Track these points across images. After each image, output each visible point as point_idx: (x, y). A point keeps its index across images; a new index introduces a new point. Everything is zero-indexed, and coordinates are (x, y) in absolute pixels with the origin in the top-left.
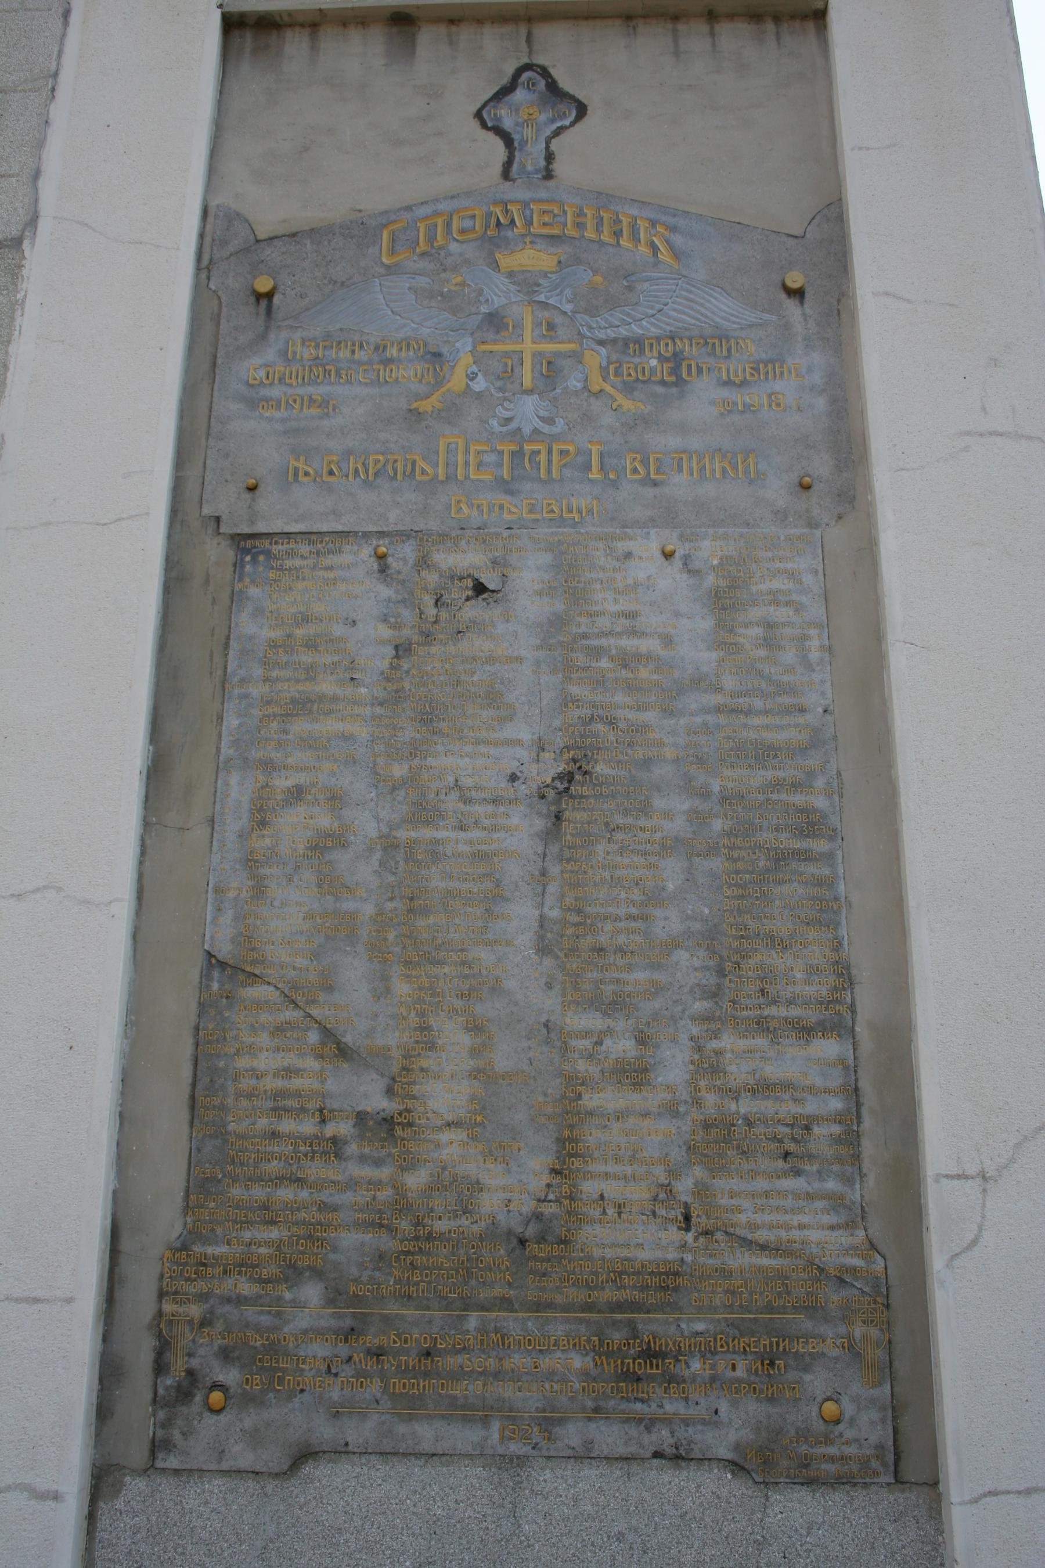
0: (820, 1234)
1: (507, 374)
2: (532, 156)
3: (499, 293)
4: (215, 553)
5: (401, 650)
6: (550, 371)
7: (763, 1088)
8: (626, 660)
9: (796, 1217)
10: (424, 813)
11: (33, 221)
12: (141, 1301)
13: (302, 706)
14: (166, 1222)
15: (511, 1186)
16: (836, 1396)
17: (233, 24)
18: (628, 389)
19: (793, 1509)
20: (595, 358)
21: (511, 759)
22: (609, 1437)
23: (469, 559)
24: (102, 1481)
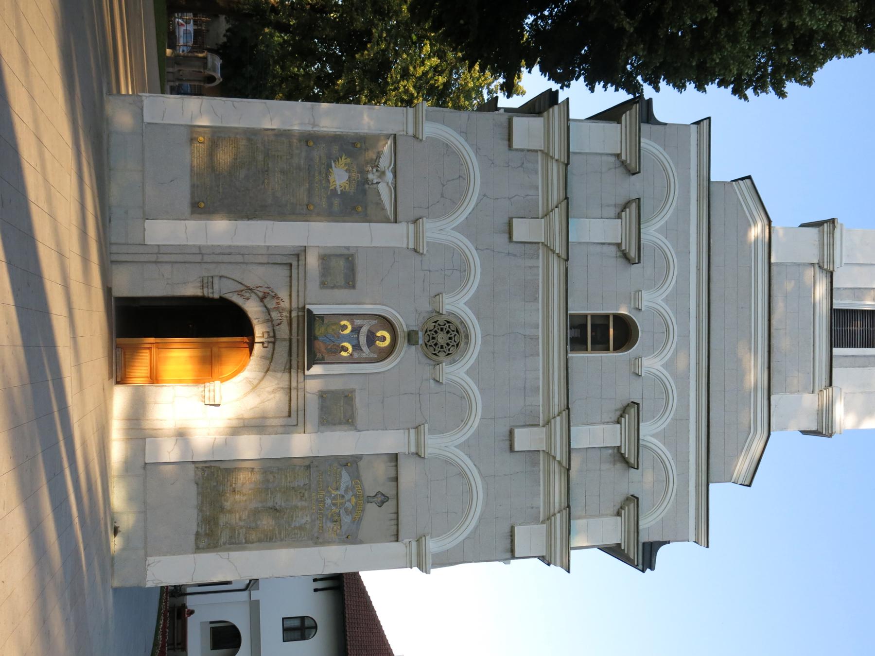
0: (223, 540)
1: (334, 498)
2: (371, 500)
3: (347, 497)
4: (307, 463)
5: (293, 488)
6: (335, 504)
7: (239, 534)
8: (292, 517)
9: (224, 537)
10: (272, 494)
11: (359, 431)
12: (213, 464)
13: (286, 476)
14: (223, 466)
15: (227, 505)
16: (203, 543)
18: (332, 515)
19: (193, 538)
20: (337, 510)
21: (279, 503)
22: (200, 517)
23: (306, 495)
24: (193, 462)
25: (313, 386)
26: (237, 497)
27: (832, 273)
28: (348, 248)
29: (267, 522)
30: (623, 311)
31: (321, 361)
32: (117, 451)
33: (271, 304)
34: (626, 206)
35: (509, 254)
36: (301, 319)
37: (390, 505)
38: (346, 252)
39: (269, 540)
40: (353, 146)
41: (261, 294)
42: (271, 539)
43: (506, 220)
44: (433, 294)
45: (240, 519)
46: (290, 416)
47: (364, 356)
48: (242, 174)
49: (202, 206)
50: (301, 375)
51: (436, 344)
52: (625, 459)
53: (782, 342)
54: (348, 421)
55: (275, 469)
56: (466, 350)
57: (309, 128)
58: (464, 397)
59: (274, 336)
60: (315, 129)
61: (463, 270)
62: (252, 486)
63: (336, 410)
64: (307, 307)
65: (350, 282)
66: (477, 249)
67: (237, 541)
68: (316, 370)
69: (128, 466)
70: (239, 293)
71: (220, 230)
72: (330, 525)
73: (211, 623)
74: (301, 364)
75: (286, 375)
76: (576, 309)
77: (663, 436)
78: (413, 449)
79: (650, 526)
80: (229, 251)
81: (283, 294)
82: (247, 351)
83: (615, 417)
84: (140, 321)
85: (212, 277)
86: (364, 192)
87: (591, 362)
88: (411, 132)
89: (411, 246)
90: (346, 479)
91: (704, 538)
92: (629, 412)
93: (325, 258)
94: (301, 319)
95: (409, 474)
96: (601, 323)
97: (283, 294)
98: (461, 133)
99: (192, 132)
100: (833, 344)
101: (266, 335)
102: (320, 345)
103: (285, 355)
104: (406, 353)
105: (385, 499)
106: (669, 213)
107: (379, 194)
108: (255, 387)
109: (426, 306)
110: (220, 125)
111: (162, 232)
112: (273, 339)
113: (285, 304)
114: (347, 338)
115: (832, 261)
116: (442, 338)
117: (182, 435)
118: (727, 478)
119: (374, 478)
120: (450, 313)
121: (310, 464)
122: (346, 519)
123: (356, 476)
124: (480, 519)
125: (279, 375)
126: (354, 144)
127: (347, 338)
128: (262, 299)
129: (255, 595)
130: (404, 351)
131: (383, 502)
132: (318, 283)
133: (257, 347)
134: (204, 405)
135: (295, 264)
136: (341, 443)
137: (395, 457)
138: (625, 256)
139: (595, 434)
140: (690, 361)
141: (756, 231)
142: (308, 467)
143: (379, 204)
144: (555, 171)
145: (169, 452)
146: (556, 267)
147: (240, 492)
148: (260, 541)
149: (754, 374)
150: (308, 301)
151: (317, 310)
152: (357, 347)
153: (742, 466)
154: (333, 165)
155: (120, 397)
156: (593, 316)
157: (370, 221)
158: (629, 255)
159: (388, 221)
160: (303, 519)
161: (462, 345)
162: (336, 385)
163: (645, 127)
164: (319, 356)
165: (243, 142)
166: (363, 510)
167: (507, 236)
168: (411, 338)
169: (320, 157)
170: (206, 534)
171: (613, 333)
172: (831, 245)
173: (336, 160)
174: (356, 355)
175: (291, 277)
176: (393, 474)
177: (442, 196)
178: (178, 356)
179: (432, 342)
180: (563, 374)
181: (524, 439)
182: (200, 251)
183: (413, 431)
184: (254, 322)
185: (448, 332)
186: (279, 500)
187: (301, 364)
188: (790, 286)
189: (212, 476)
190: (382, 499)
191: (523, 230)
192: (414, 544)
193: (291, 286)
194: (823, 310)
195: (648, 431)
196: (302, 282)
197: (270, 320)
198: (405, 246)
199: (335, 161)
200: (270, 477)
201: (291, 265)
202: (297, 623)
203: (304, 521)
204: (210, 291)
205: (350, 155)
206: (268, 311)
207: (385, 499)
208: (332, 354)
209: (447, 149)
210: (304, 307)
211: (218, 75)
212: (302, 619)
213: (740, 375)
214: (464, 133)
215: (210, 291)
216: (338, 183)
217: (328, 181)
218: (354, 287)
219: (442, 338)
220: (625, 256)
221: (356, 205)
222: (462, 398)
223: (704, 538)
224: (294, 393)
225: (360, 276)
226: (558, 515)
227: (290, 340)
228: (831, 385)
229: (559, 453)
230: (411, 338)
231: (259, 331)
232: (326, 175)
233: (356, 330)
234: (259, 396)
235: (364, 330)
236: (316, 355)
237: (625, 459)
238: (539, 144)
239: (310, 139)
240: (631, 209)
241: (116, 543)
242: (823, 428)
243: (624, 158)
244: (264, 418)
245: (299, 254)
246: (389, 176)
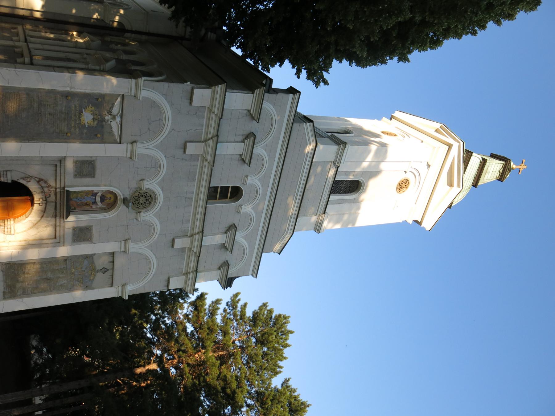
0: (18, 294)
4: (65, 258)
14: (17, 263)
17: (114, 253)
23: (65, 272)
26: (26, 276)
27: (338, 167)
28: (91, 157)
29: (43, 286)
33: (44, 185)
34: (247, 137)
35: (182, 159)
36: (62, 193)
37: (109, 273)
38: (90, 159)
41: (38, 179)
42: (45, 291)
43: (183, 142)
44: (139, 179)
45: (28, 284)
46: (55, 238)
47: (98, 207)
48: (24, 115)
50: (62, 220)
51: (139, 203)
55: (47, 264)
56: (154, 205)
57: (68, 89)
58: (151, 226)
59: (46, 200)
60: (72, 90)
62: (35, 270)
63: (82, 234)
64: (66, 189)
65: (91, 174)
66: (165, 157)
67: (25, 293)
70: (24, 179)
72: (77, 282)
74: (62, 215)
75: (53, 219)
78: (122, 250)
82: (29, 203)
83: (224, 230)
85: (6, 171)
86: (102, 127)
88: (133, 94)
89: (129, 156)
92: (232, 228)
94: (62, 193)
95: (119, 261)
98: (163, 95)
101: (41, 200)
103: (53, 209)
104: (121, 209)
105: (107, 270)
107: (111, 128)
108: (35, 225)
109: (134, 185)
110: (7, 85)
112: (46, 201)
116: (142, 200)
119: (101, 263)
120: (147, 189)
121: (66, 259)
124: (153, 276)
125: (49, 219)
126: (97, 99)
128: (38, 182)
131: (105, 272)
132: (72, 175)
133: (36, 206)
135: (58, 164)
136: (84, 249)
137: (113, 253)
138: (243, 161)
139: (214, 239)
140: (265, 205)
142: (66, 260)
143: (111, 133)
147: (27, 273)
148: (39, 292)
149: (292, 211)
150: (66, 184)
151: (71, 189)
153: (278, 247)
154: (83, 110)
157: (104, 143)
159: (115, 142)
160: (62, 282)
161: (153, 203)
163: (267, 95)
164: (72, 208)
165: (24, 96)
166: (95, 276)
167: (183, 150)
169: (75, 106)
170: (9, 292)
172: (342, 155)
173: (85, 108)
174: (94, 206)
175: (56, 170)
176: (111, 260)
177: (149, 129)
179: (136, 202)
180: (203, 216)
183: (123, 243)
184: (34, 193)
185: (145, 197)
186: (49, 275)
187: (62, 215)
188: (319, 169)
192: (120, 288)
193: (56, 176)
194: (330, 181)
196: (63, 175)
197: (43, 192)
198: (125, 156)
199: (84, 109)
200: (45, 266)
201: (56, 165)
203: (63, 282)
204: (5, 179)
205: (94, 105)
206: (43, 188)
207: (107, 270)
209: (154, 104)
210: (64, 188)
214: (165, 95)
215: (5, 179)
216: (86, 121)
217: (80, 120)
218: (94, 177)
219: (141, 200)
220: (243, 161)
221: (97, 133)
222: (150, 226)
224: (58, 228)
225: (98, 172)
226: (191, 274)
227: (56, 203)
228: (324, 213)
229: (195, 248)
231: (36, 197)
232: (79, 117)
234: (37, 229)
235: (99, 195)
236: (70, 207)
239: (67, 95)
242: (318, 228)
243: (251, 113)
244: (42, 239)
245: (62, 160)
246: (118, 119)
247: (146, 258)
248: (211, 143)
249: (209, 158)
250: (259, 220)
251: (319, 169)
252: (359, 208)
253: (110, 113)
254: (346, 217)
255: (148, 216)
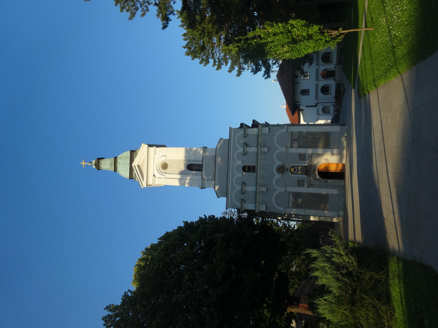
25: (307, 162)
29: (317, 137)
30: (244, 173)
31: (305, 166)
32: (345, 152)
34: (244, 193)
39: (316, 133)
40: (297, 206)
49: (327, 196)
52: (246, 145)
53: (212, 165)
54: (300, 155)
55: (315, 146)
56: (277, 166)
61: (277, 182)
63: (302, 157)
67: (323, 133)
68: (306, 165)
69: (343, 149)
70: (320, 180)
71: (324, 191)
73: (328, 94)
76: (254, 174)
77: (238, 149)
79: (242, 132)
80: (322, 187)
81: (312, 179)
84: (339, 175)
87: (251, 163)
90: (301, 144)
91: (230, 128)
92: (245, 154)
93: (303, 185)
95: (289, 144)
96: (249, 171)
97: (312, 179)
99: (328, 210)
100: (202, 165)
102: (305, 169)
104: (288, 167)
106: (235, 192)
111: (335, 192)
112: (314, 171)
113: (311, 177)
114: (299, 170)
115: (202, 181)
116: (281, 169)
117: (333, 154)
118: (225, 140)
119: (296, 145)
121: (308, 147)
122: (301, 136)
123: (299, 144)
127: (299, 170)
128: (316, 178)
129: (316, 101)
130: (289, 168)
134: (329, 160)
136: (302, 151)
137: (291, 147)
138: (244, 184)
139: (252, 150)
141: (217, 188)
143: (292, 195)
144: (258, 200)
145: (335, 151)
146: (258, 182)
149: (219, 159)
151: (305, 176)
152: (298, 168)
155: (344, 162)
156: (250, 172)
158: (244, 183)
162: (303, 162)
168: (287, 170)
171: (247, 169)
178: (333, 169)
181: (266, 150)
182: (327, 188)
189: (327, 146)
190: (294, 140)
191: (264, 189)
194: (204, 172)
195: (241, 150)
197: (315, 174)
202: (305, 94)
207: (293, 140)
208: (303, 167)
211: (320, 239)
212: (304, 95)
213: (221, 160)
219: (281, 169)
220: (244, 184)
221: (297, 195)
223: (230, 128)
229: (259, 147)
230: (287, 170)
231: (317, 173)
233: (298, 172)
237: (246, 145)
238: (261, 205)
239: (305, 208)
240: (243, 192)
241: (346, 135)
242: (205, 148)
245: (308, 186)
246: (290, 200)
247: (278, 143)
248: (258, 192)
249: (258, 186)
250: (233, 157)
251: (210, 177)
252: (185, 157)
253: (293, 202)
254: (192, 153)
255: (279, 163)
